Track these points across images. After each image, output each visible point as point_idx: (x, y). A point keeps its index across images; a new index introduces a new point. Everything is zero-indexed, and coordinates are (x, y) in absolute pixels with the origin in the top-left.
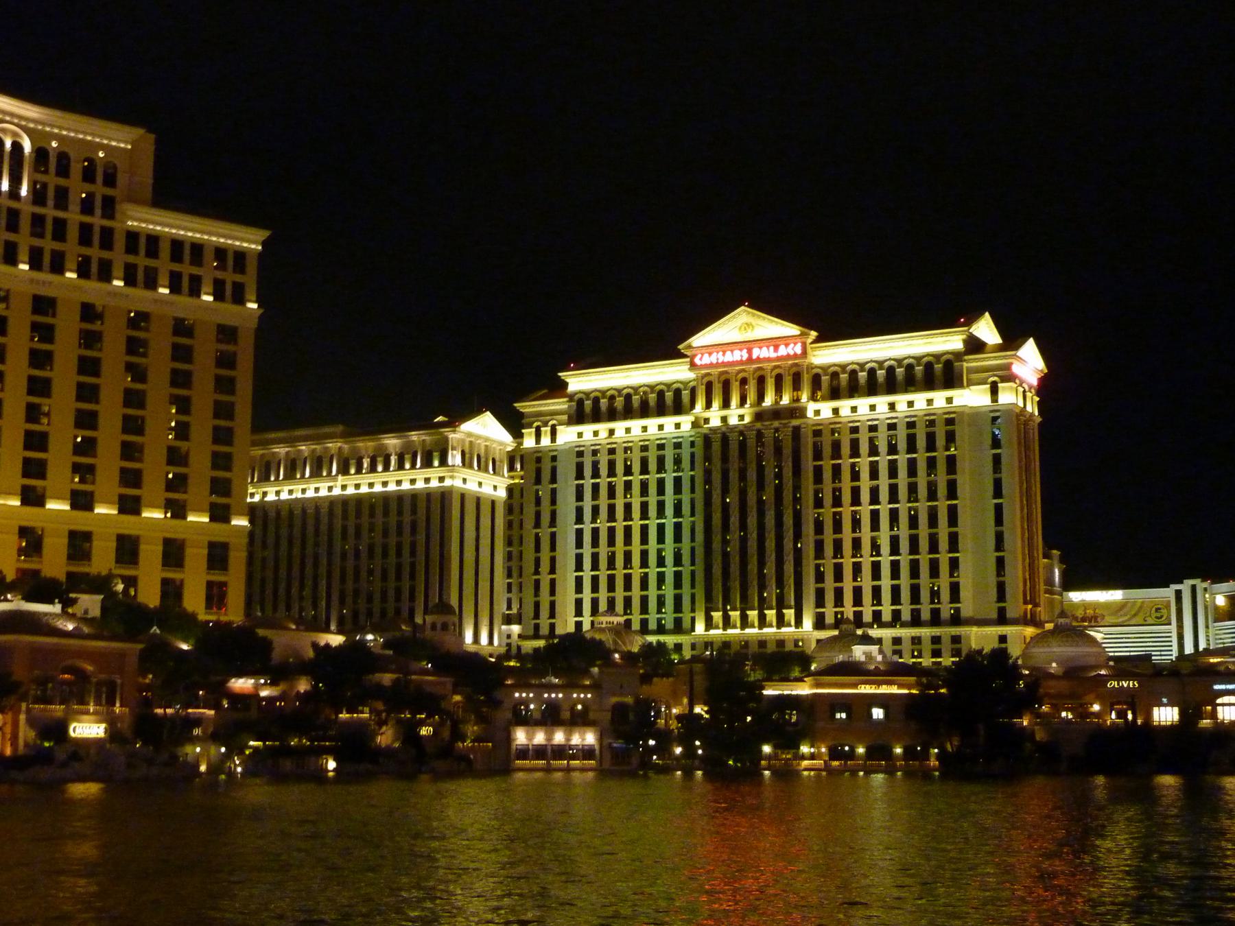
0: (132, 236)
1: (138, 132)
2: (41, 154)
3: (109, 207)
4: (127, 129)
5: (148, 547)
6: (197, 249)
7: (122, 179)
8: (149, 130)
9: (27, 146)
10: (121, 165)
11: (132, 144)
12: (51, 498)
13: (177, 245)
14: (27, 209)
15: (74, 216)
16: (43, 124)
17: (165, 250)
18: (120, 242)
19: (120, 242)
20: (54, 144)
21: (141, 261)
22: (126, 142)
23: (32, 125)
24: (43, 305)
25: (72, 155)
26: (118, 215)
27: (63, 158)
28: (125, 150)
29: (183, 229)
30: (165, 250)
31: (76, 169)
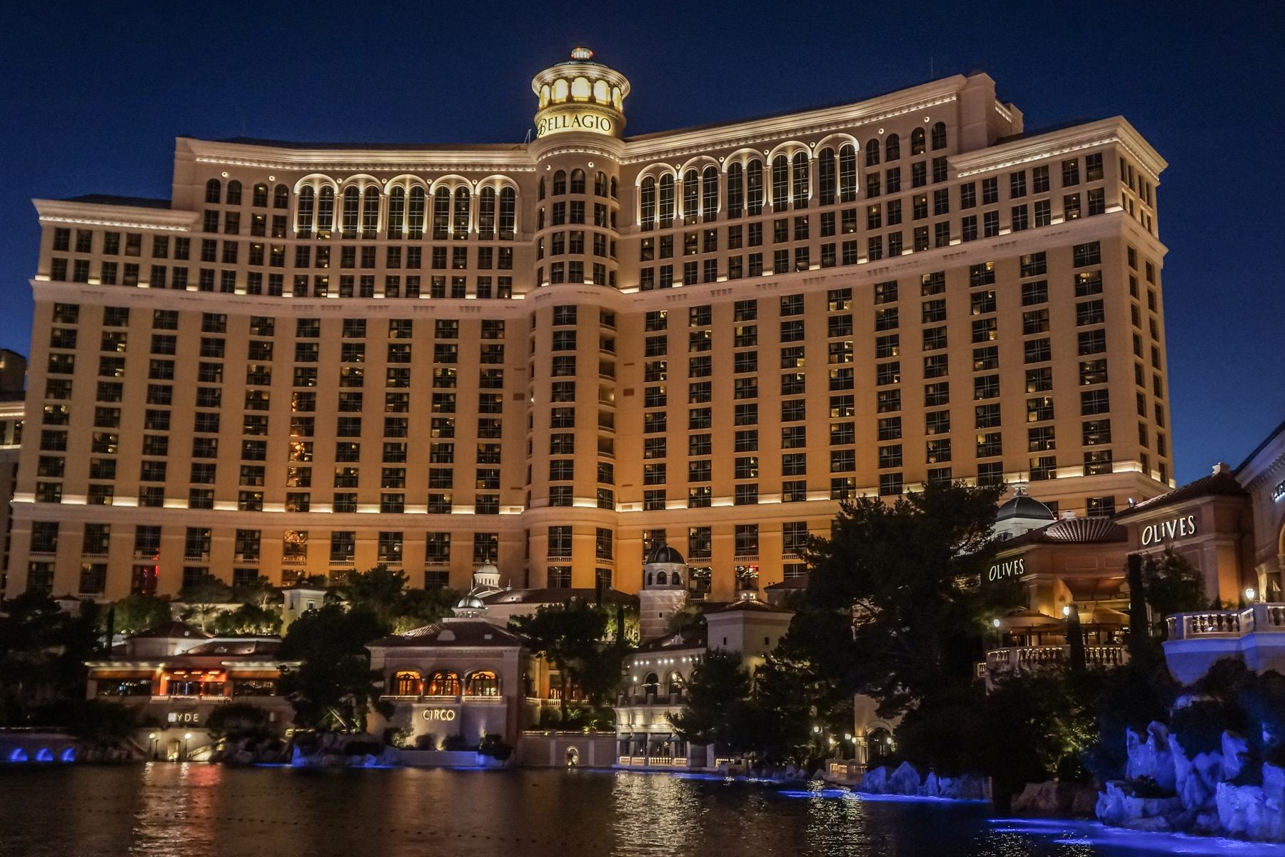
0: (968, 188)
2: (871, 149)
3: (941, 170)
4: (942, 82)
5: (269, 541)
6: (1041, 172)
10: (950, 121)
11: (958, 96)
16: (870, 117)
18: (955, 200)
19: (955, 200)
20: (882, 132)
22: (950, 96)
23: (858, 124)
24: (308, 327)
27: (893, 141)
29: (1018, 158)
31: (905, 145)
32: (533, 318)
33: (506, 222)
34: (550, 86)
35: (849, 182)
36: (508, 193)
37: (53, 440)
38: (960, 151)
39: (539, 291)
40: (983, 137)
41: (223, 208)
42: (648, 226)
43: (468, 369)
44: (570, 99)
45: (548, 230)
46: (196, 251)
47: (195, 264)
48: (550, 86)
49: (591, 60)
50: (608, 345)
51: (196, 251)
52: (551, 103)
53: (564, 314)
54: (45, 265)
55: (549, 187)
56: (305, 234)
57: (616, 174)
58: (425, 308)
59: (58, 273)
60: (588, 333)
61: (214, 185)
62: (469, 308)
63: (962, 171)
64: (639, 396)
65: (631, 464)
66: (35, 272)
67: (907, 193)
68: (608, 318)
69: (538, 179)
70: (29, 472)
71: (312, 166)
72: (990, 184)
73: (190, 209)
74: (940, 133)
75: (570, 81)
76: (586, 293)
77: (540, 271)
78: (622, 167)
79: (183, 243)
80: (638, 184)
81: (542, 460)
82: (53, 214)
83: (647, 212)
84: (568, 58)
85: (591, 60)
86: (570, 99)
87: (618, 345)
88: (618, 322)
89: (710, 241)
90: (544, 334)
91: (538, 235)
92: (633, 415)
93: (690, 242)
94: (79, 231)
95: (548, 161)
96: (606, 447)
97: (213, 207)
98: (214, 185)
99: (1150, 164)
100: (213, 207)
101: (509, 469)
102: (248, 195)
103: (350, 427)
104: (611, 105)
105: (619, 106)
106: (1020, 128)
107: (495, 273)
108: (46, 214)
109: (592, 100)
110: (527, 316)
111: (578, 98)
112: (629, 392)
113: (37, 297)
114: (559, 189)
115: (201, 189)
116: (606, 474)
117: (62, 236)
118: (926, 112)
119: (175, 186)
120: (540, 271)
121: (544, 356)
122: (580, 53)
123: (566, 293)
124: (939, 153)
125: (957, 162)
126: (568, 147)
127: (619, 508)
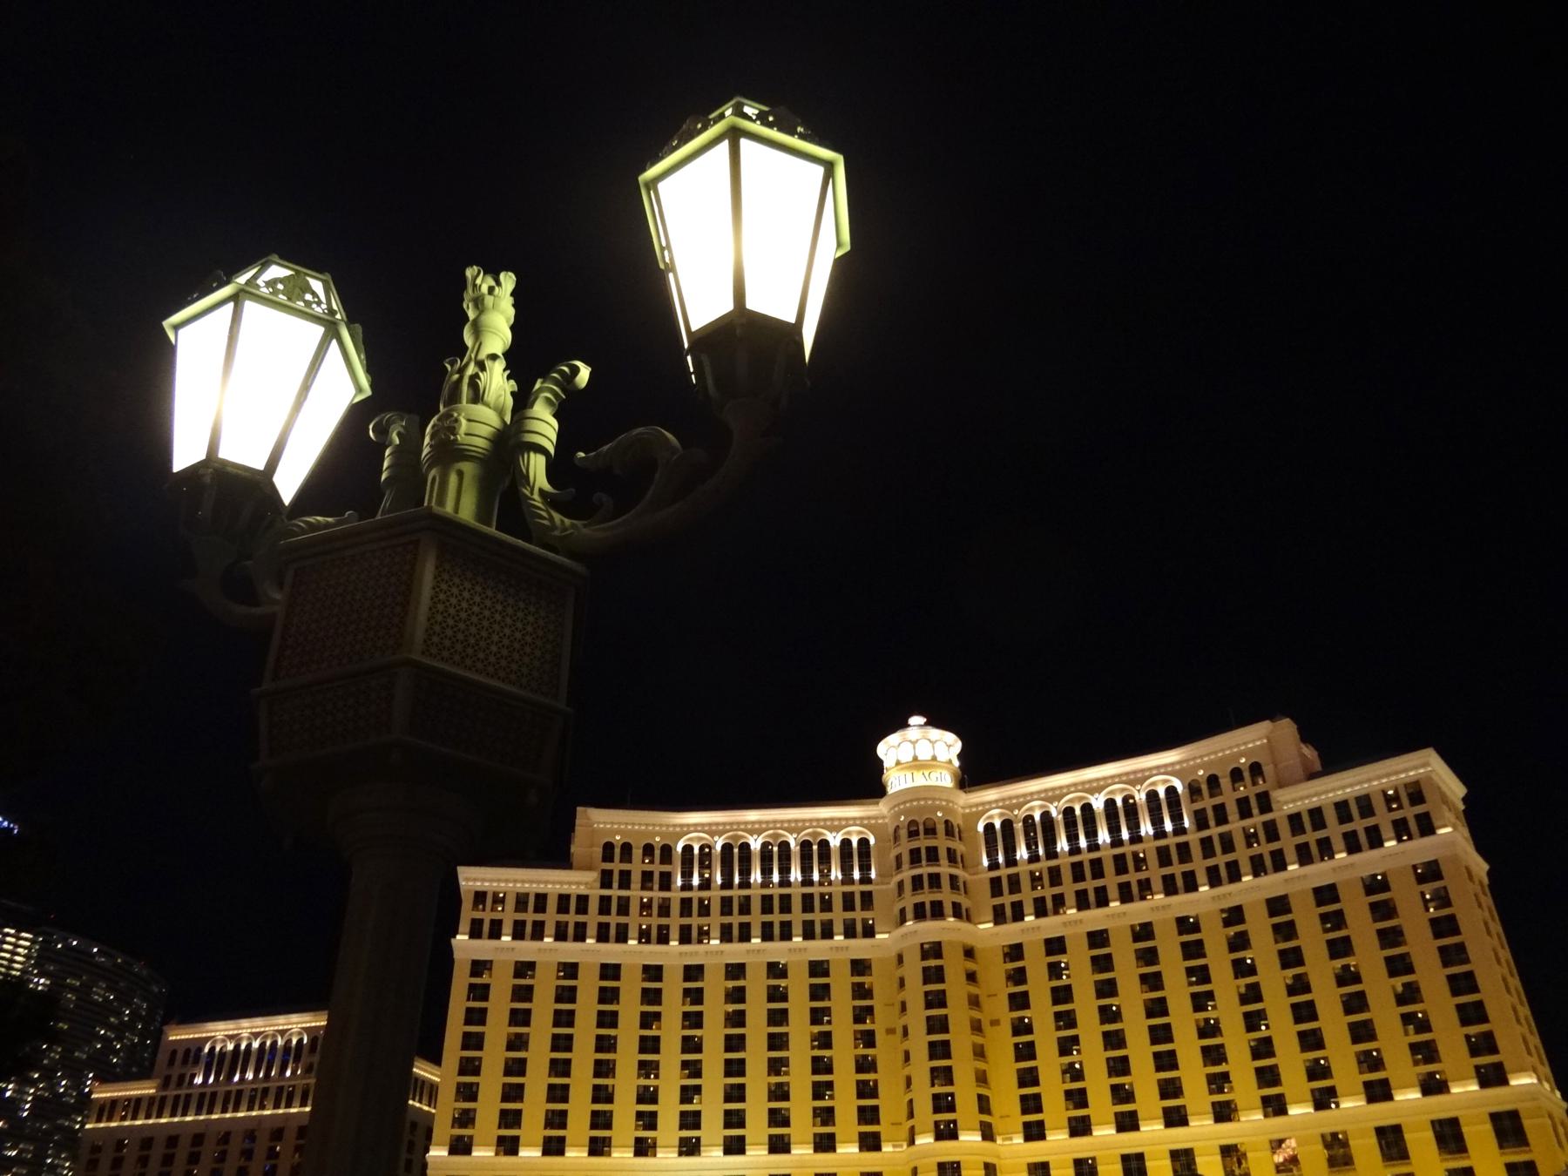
0: (1295, 820)
1: (1263, 727)
2: (1194, 790)
3: (1265, 803)
7: (1268, 769)
8: (1271, 716)
9: (1180, 789)
12: (1296, 1103)
13: (1342, 808)
14: (1193, 838)
15: (1235, 825)
17: (1330, 816)
18: (1284, 829)
19: (1284, 829)
20: (1201, 773)
21: (1311, 837)
25: (1219, 774)
26: (1274, 806)
27: (1213, 781)
28: (1262, 746)
30: (1330, 816)
31: (1225, 783)
32: (900, 959)
33: (865, 868)
34: (891, 749)
35: (1177, 818)
36: (863, 842)
37: (468, 1093)
38: (1281, 785)
39: (903, 930)
40: (1300, 772)
41: (616, 866)
42: (994, 866)
43: (841, 1003)
44: (915, 759)
45: (907, 874)
46: (594, 906)
47: (593, 919)
48: (891, 749)
49: (926, 724)
50: (971, 977)
51: (594, 906)
52: (898, 763)
53: (933, 950)
54: (465, 925)
55: (903, 833)
56: (687, 887)
57: (961, 822)
58: (797, 951)
59: (475, 933)
60: (954, 967)
61: (608, 848)
62: (839, 948)
63: (1286, 803)
64: (1007, 1028)
65: (1006, 1096)
66: (455, 932)
67: (1235, 825)
68: (969, 953)
69: (891, 830)
70: (443, 1129)
71: (696, 826)
72: (1316, 814)
73: (589, 868)
74: (1256, 769)
75: (914, 743)
76: (946, 929)
77: (903, 911)
78: (964, 815)
79: (583, 901)
80: (981, 828)
81: (923, 1094)
82: (472, 879)
83: (992, 854)
84: (905, 725)
85: (926, 724)
86: (915, 759)
87: (979, 977)
88: (978, 955)
89: (1055, 876)
90: (914, 969)
91: (898, 878)
92: (1002, 1043)
93: (1035, 880)
94: (1406, 786)
95: (906, 812)
96: (982, 1078)
97: (608, 866)
98: (608, 848)
99: (1455, 789)
100: (608, 866)
101: (889, 1103)
102: (637, 853)
103: (735, 1068)
104: (950, 762)
105: (956, 763)
106: (1318, 767)
107: (858, 915)
108: (467, 879)
109: (934, 758)
110: (894, 954)
111: (918, 755)
112: (995, 1023)
113: (457, 955)
114: (913, 834)
115: (598, 851)
116: (984, 1104)
117: (480, 897)
118: (1242, 754)
119: (573, 849)
120: (903, 911)
121: (916, 991)
122: (917, 720)
123: (930, 930)
124: (1261, 786)
125: (1278, 796)
126: (918, 800)
127: (999, 1141)
